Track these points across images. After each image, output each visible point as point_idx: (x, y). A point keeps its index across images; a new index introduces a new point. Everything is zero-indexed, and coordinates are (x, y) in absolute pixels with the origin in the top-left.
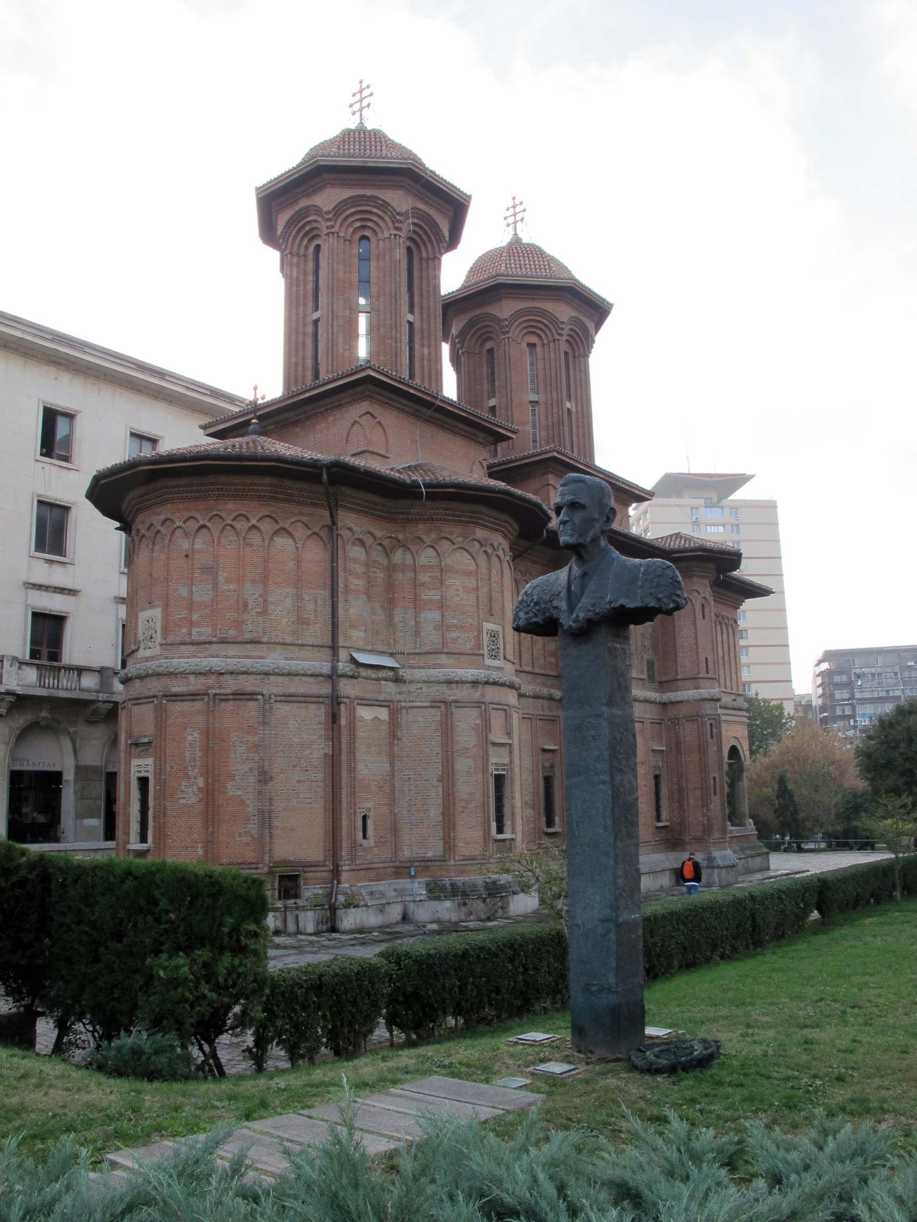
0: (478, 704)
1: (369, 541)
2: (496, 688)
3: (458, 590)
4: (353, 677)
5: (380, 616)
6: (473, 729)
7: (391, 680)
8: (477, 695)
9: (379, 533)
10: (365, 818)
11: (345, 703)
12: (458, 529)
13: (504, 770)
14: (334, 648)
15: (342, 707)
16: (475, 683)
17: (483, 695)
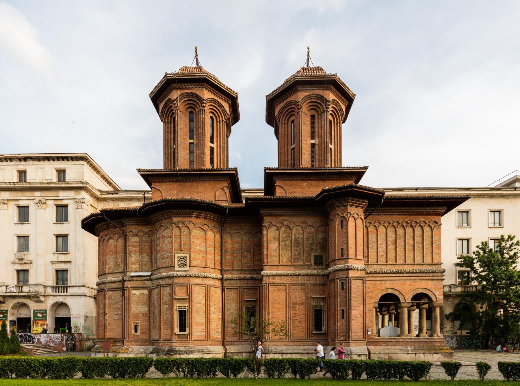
0: (170, 285)
1: (141, 234)
2: (182, 278)
3: (166, 244)
4: (130, 281)
5: (146, 259)
6: (168, 294)
7: (149, 280)
8: (171, 282)
9: (146, 230)
10: (136, 326)
11: (126, 289)
12: (167, 221)
13: (186, 309)
14: (125, 272)
15: (125, 291)
16: (170, 277)
17: (173, 282)
